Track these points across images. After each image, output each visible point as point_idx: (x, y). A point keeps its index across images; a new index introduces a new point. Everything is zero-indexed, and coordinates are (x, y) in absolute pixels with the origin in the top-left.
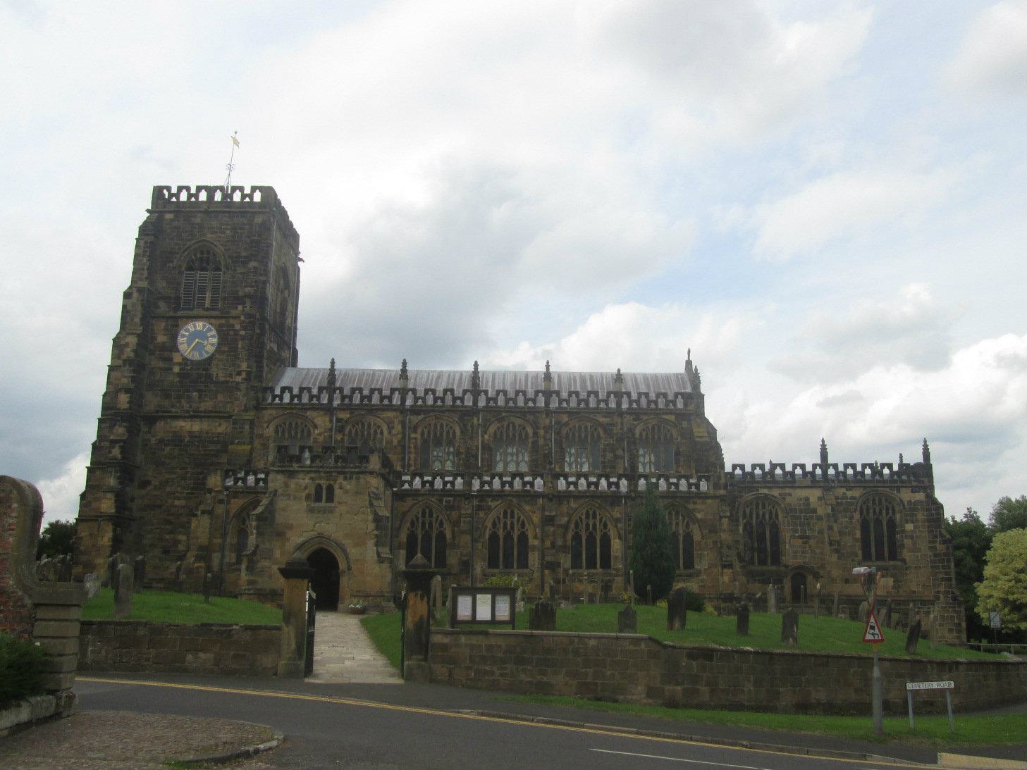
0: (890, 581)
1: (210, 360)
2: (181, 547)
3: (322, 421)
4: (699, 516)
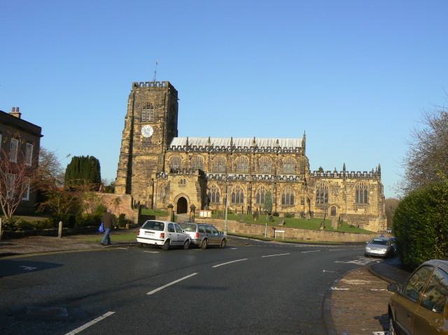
0: (363, 210)
1: (151, 137)
2: (144, 194)
3: (184, 155)
4: (295, 188)
